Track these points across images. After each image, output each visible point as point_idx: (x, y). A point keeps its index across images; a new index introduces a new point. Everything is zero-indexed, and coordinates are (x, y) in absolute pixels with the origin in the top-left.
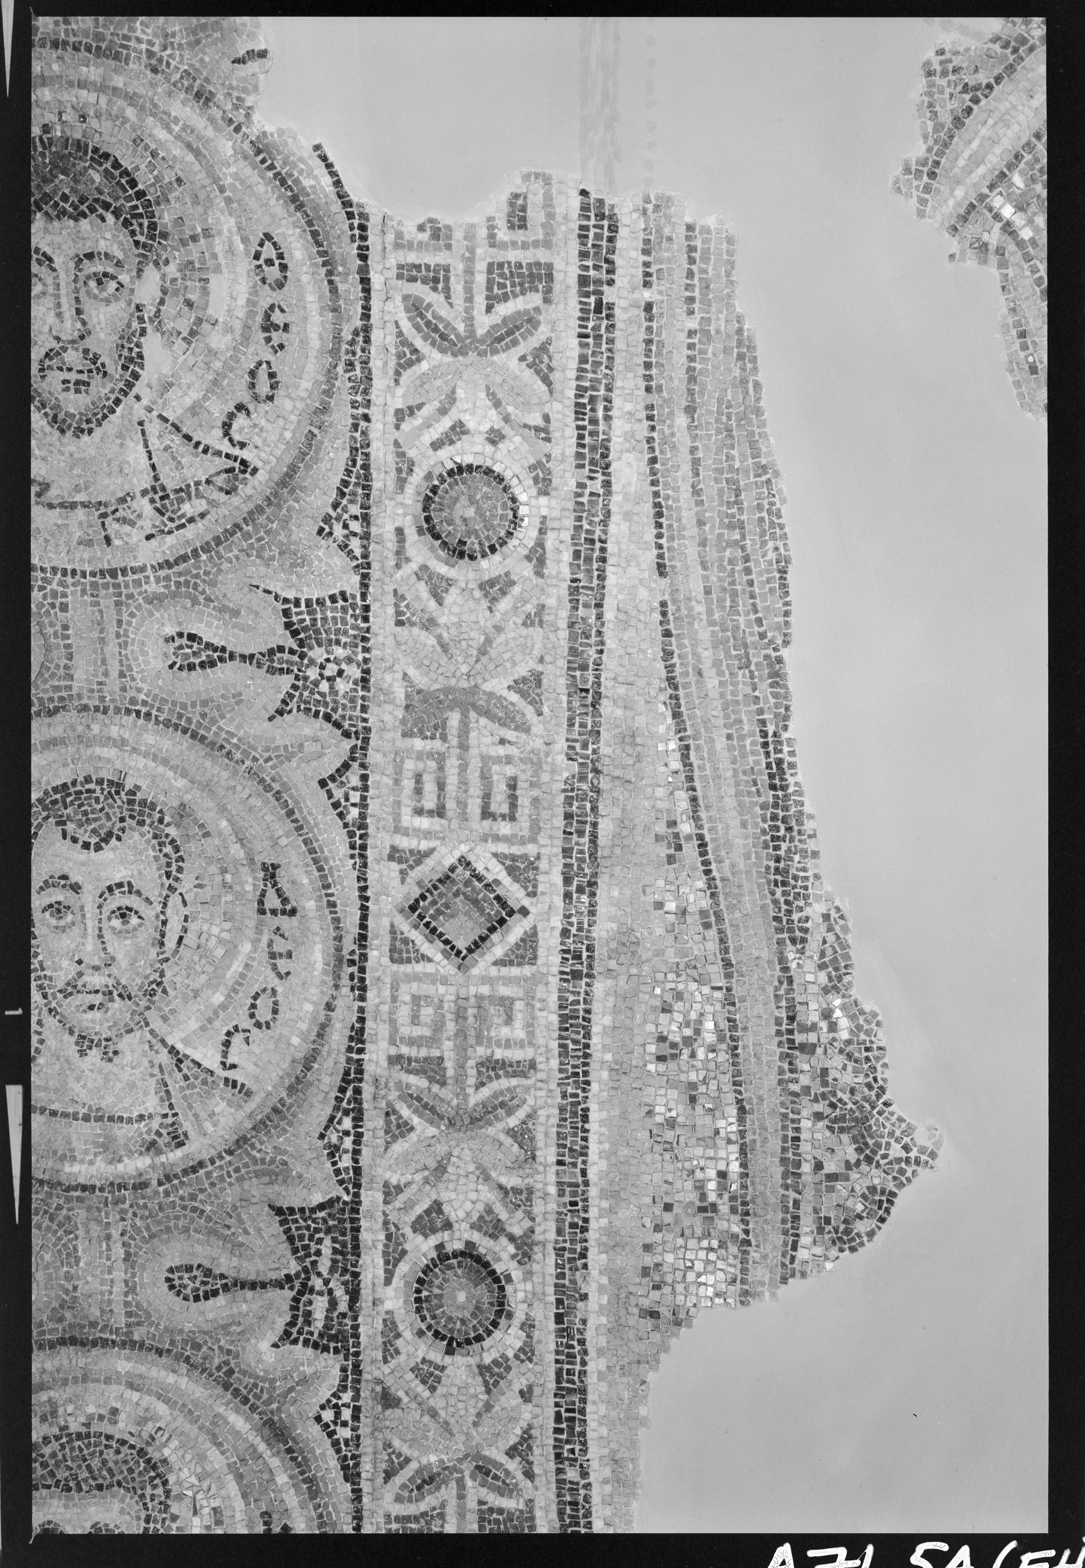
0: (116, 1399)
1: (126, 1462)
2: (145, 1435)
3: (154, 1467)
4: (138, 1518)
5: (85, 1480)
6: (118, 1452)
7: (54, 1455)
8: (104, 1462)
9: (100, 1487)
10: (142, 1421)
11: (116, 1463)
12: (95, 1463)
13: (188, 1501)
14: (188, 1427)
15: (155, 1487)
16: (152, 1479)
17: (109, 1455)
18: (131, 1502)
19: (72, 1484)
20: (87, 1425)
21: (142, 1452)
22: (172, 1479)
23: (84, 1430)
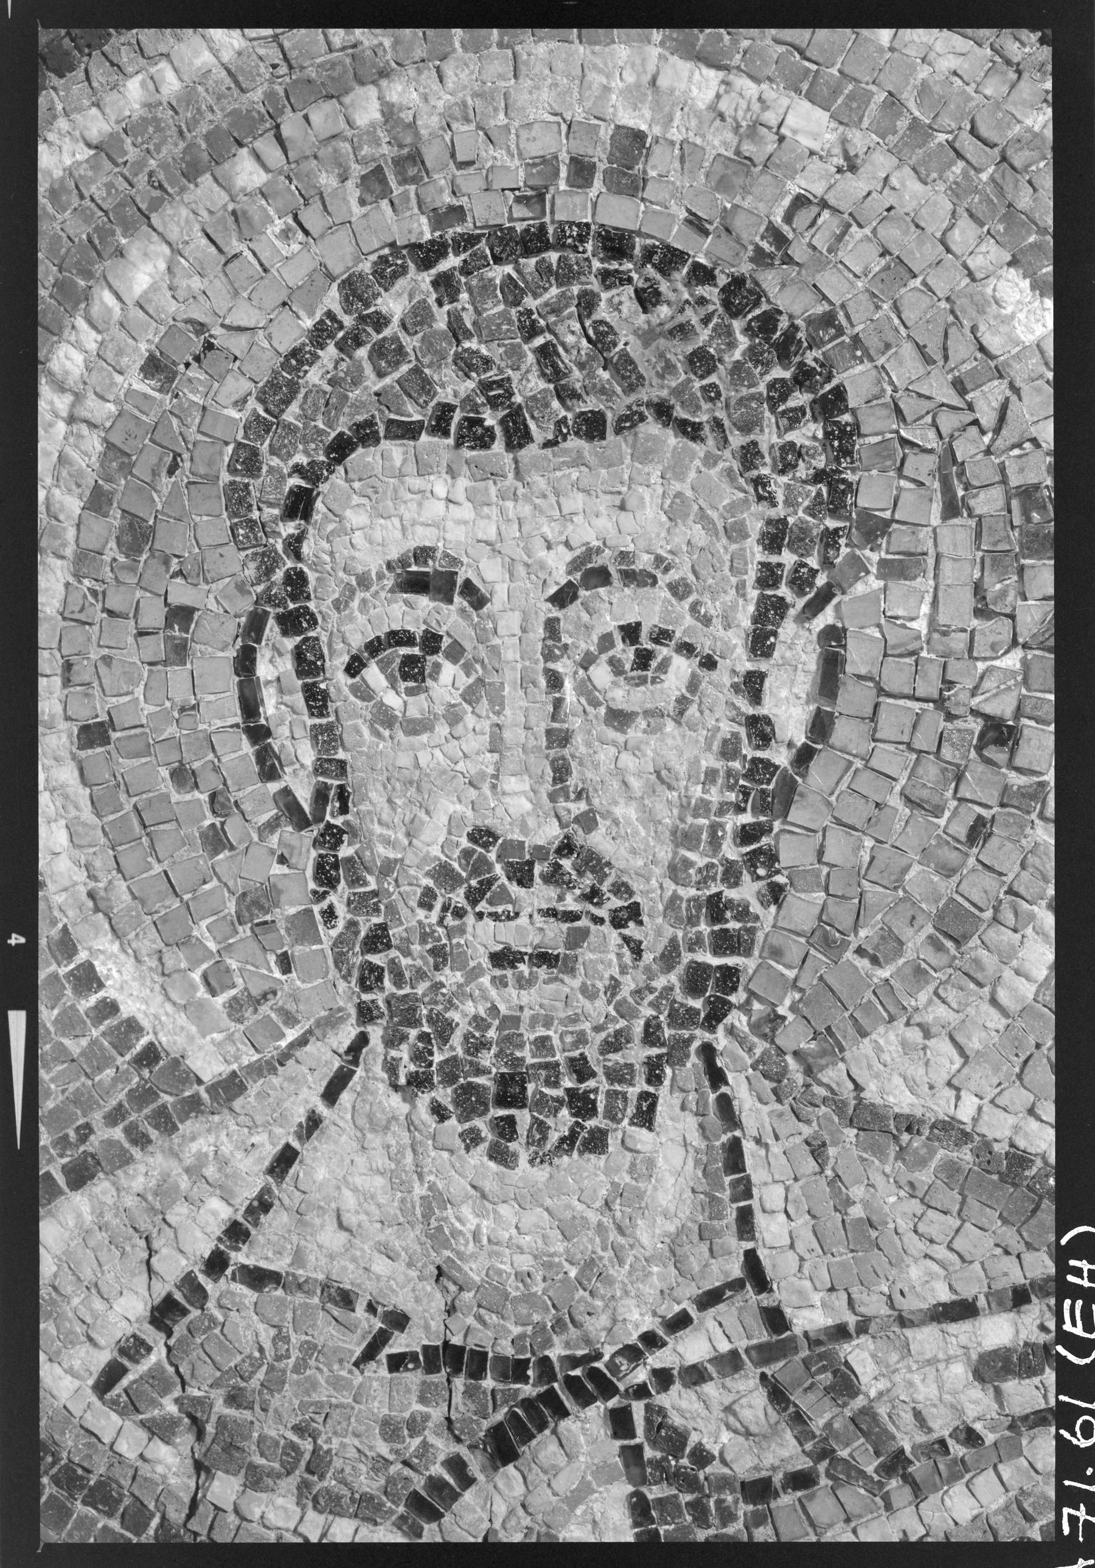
0: (633, 96)
1: (683, 331)
2: (754, 236)
3: (786, 348)
4: (736, 532)
5: (538, 402)
6: (647, 299)
7: (419, 317)
8: (601, 338)
9: (593, 427)
10: (739, 168)
11: (647, 337)
12: (572, 335)
13: (921, 466)
14: (911, 190)
15: (794, 418)
16: (780, 391)
17: (618, 309)
18: (707, 474)
19: (490, 419)
20: (536, 198)
21: (739, 295)
22: (856, 379)
23: (522, 219)
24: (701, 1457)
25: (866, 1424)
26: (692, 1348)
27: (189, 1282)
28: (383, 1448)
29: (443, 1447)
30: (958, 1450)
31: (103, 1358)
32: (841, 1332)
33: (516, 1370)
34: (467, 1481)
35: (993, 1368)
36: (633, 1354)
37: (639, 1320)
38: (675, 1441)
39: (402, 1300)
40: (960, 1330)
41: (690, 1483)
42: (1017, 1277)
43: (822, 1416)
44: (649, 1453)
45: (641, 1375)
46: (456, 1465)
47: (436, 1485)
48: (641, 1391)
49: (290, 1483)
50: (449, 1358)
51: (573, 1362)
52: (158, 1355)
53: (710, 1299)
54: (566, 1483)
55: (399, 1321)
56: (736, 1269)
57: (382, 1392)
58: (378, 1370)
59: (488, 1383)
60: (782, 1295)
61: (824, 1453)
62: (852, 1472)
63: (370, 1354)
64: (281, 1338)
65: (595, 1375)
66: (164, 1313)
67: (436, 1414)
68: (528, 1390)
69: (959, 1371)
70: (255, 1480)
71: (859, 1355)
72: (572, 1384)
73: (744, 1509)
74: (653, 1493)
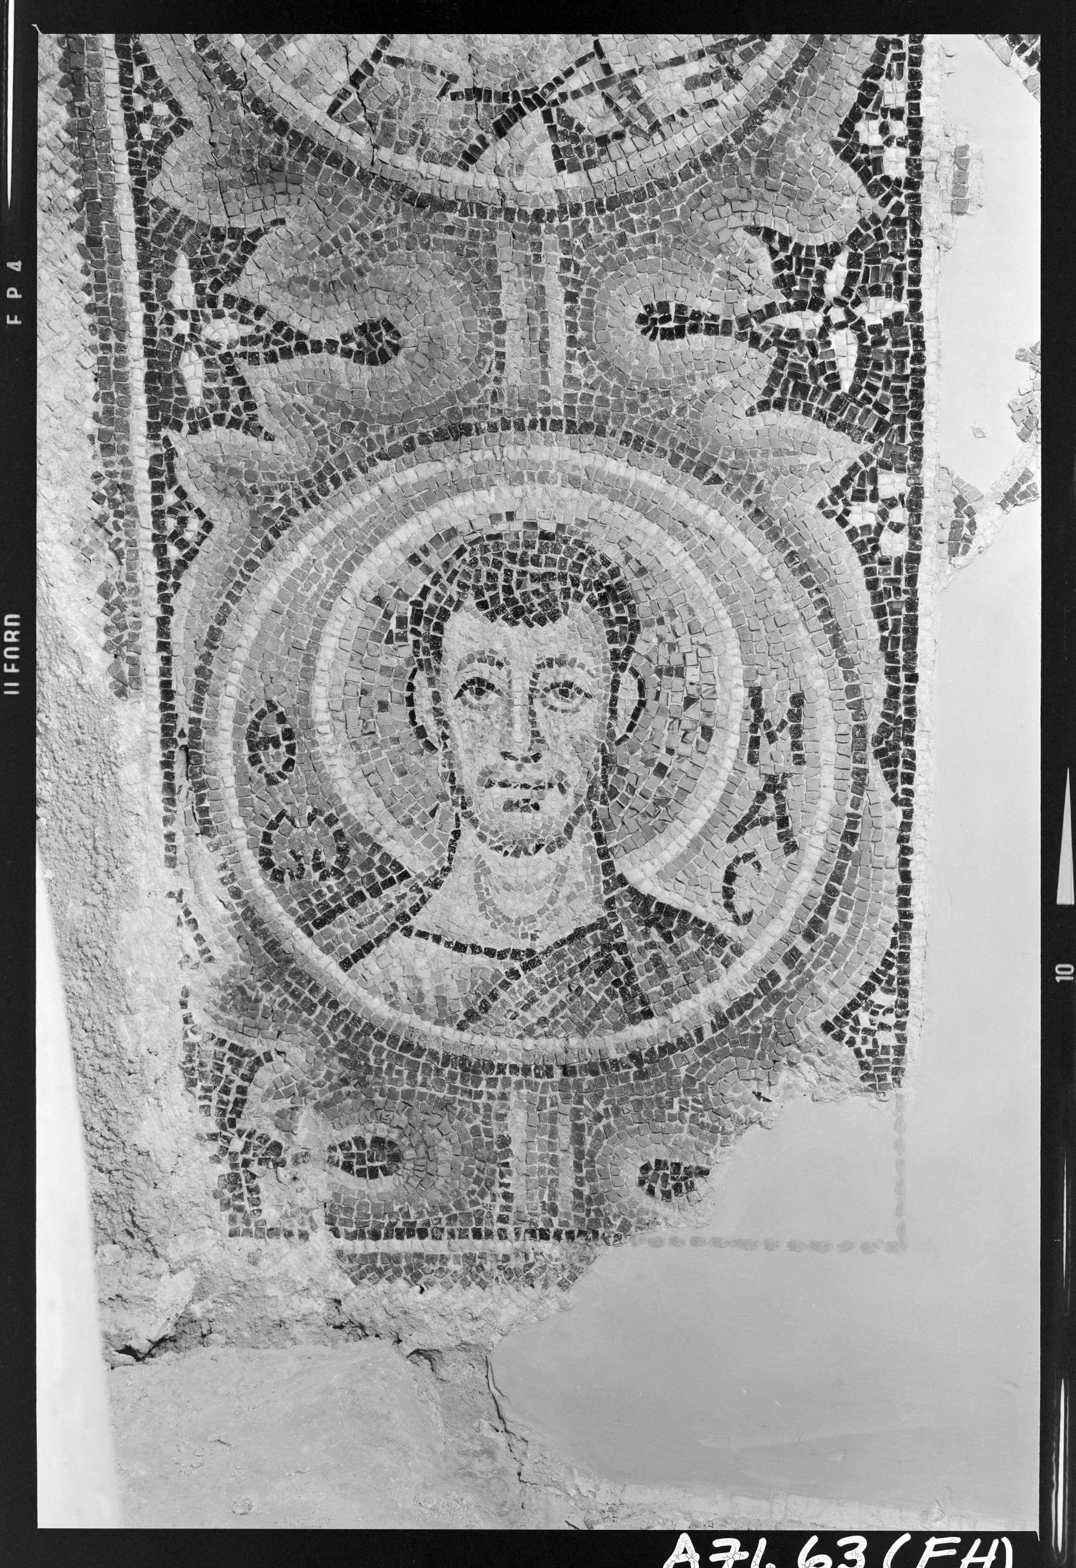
24: (580, 128)
25: (644, 110)
26: (574, 83)
27: (365, 63)
28: (451, 133)
29: (476, 132)
30: (678, 118)
31: (329, 100)
32: (632, 73)
33: (504, 97)
34: (486, 145)
35: (692, 83)
36: (550, 87)
37: (553, 72)
38: (569, 122)
39: (455, 70)
40: (679, 69)
41: (576, 139)
42: (700, 46)
43: (623, 103)
44: (559, 128)
45: (555, 96)
46: (482, 139)
47: (474, 148)
48: (555, 103)
49: (413, 150)
50: (475, 93)
51: (526, 92)
52: (354, 97)
53: (581, 62)
54: (526, 143)
55: (454, 78)
56: (591, 49)
57: (449, 110)
58: (447, 99)
59: (493, 103)
60: (609, 58)
61: (627, 123)
62: (637, 131)
63: (443, 93)
64: (406, 87)
65: (536, 97)
66: (356, 79)
67: (472, 117)
68: (510, 105)
69: (679, 86)
70: (399, 150)
71: (639, 82)
72: (527, 102)
73: (597, 148)
74: (561, 144)
